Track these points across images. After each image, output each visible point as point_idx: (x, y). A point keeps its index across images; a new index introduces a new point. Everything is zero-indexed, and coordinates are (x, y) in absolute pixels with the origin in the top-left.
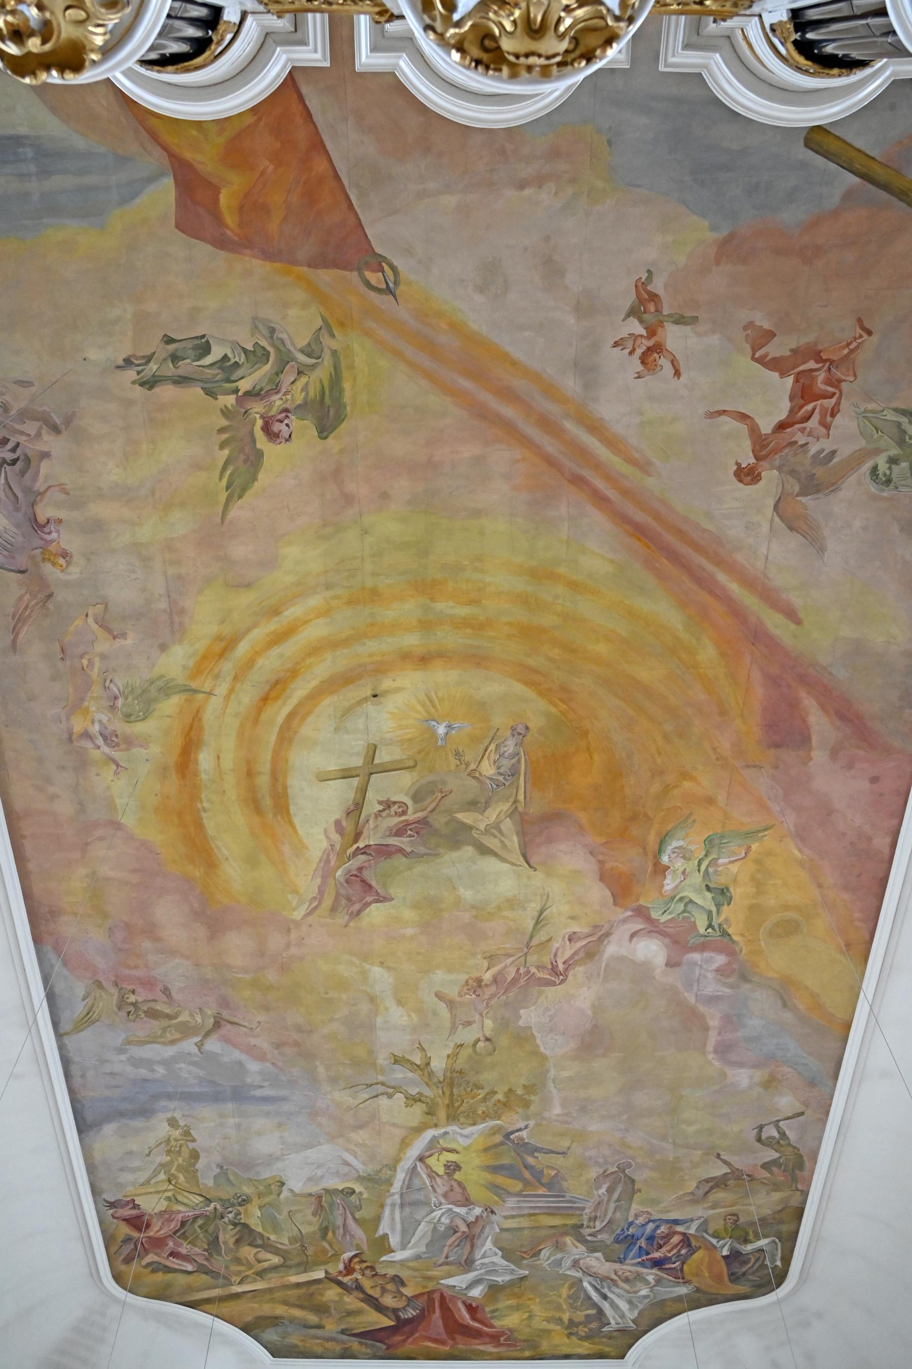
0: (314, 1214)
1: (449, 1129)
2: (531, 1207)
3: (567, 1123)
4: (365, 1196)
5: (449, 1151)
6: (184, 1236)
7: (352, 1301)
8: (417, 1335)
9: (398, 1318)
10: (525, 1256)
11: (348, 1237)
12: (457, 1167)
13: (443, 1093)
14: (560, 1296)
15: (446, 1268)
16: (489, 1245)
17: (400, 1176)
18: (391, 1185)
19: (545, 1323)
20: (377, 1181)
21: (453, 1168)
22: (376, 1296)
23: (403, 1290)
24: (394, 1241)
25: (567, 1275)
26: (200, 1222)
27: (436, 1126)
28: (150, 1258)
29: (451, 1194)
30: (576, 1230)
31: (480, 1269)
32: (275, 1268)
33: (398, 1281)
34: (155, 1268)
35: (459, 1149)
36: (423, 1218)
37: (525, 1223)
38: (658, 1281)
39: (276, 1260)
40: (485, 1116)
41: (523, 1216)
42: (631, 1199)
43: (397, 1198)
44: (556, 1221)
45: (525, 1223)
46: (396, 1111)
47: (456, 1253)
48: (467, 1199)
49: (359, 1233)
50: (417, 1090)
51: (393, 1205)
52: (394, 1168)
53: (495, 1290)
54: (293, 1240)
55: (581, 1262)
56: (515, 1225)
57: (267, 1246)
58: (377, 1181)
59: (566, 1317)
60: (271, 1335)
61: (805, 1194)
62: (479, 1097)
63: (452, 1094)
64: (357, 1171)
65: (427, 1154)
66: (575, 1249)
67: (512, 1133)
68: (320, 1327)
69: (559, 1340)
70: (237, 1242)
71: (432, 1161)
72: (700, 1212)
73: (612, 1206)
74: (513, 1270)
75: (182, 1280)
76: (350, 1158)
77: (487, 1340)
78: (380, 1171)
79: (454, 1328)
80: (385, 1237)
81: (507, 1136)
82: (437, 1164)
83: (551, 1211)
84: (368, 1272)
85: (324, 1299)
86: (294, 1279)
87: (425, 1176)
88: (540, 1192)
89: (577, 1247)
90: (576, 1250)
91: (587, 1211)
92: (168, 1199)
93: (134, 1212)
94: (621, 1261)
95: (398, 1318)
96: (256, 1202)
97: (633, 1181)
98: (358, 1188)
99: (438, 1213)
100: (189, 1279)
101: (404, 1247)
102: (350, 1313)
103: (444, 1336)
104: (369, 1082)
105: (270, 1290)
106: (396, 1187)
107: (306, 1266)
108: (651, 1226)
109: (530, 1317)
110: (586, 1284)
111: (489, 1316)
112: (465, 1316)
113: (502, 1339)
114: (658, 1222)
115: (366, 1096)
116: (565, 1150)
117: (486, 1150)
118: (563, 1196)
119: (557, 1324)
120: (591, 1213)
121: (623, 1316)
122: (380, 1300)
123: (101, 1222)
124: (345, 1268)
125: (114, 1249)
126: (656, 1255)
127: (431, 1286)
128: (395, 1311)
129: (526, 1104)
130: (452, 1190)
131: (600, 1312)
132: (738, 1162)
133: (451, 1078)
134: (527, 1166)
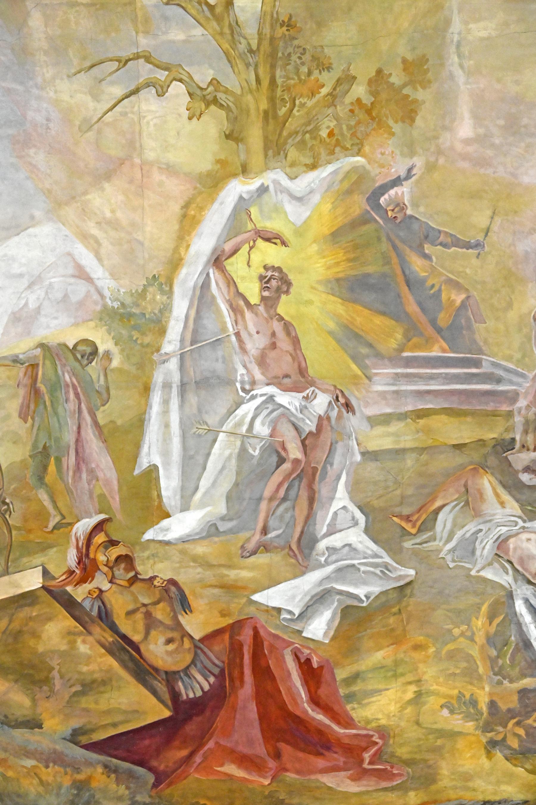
0: (24, 415)
1: (268, 178)
2: (420, 394)
3: (481, 162)
4: (115, 363)
5: (271, 238)
7: (91, 654)
8: (211, 744)
10: (408, 527)
11: (84, 476)
13: (258, 81)
14: (472, 639)
15: (262, 559)
17: (181, 306)
18: (162, 332)
19: (445, 712)
20: (136, 322)
21: (276, 283)
22: (136, 638)
23: (184, 620)
24: (169, 486)
25: (485, 580)
27: (244, 170)
29: (272, 354)
31: (327, 563)
33: (176, 596)
35: (287, 233)
36: (222, 422)
40: (336, 145)
41: (402, 417)
43: (173, 364)
46: (173, 131)
47: (282, 517)
48: (302, 371)
50: (210, 74)
51: (167, 386)
52: (165, 283)
53: (354, 620)
55: (512, 543)
56: (387, 444)
58: (136, 322)
62: (324, 91)
63: (273, 82)
64: (102, 296)
65: (228, 247)
66: (499, 510)
67: (384, 189)
68: (34, 724)
74: (386, 566)
76: (87, 259)
77: (341, 760)
78: (143, 294)
80: (153, 469)
83: (453, 403)
84: (120, 572)
85: (41, 649)
87: (224, 307)
88: (435, 352)
89: (502, 504)
91: (522, 403)
98: (104, 343)
99: (247, 409)
101: (185, 508)
102: (89, 687)
103: (260, 749)
104: (124, 54)
106: (171, 343)
109: (418, 699)
110: (520, 606)
111: (342, 691)
113: (367, 756)
115: (118, 91)
116: (480, 237)
117: (335, 236)
118: (477, 363)
119: (468, 717)
120: (528, 407)
122: (142, 648)
124: (80, 562)
127: (237, 610)
128: (170, 678)
129: (409, 112)
130: (274, 346)
133: (272, 39)
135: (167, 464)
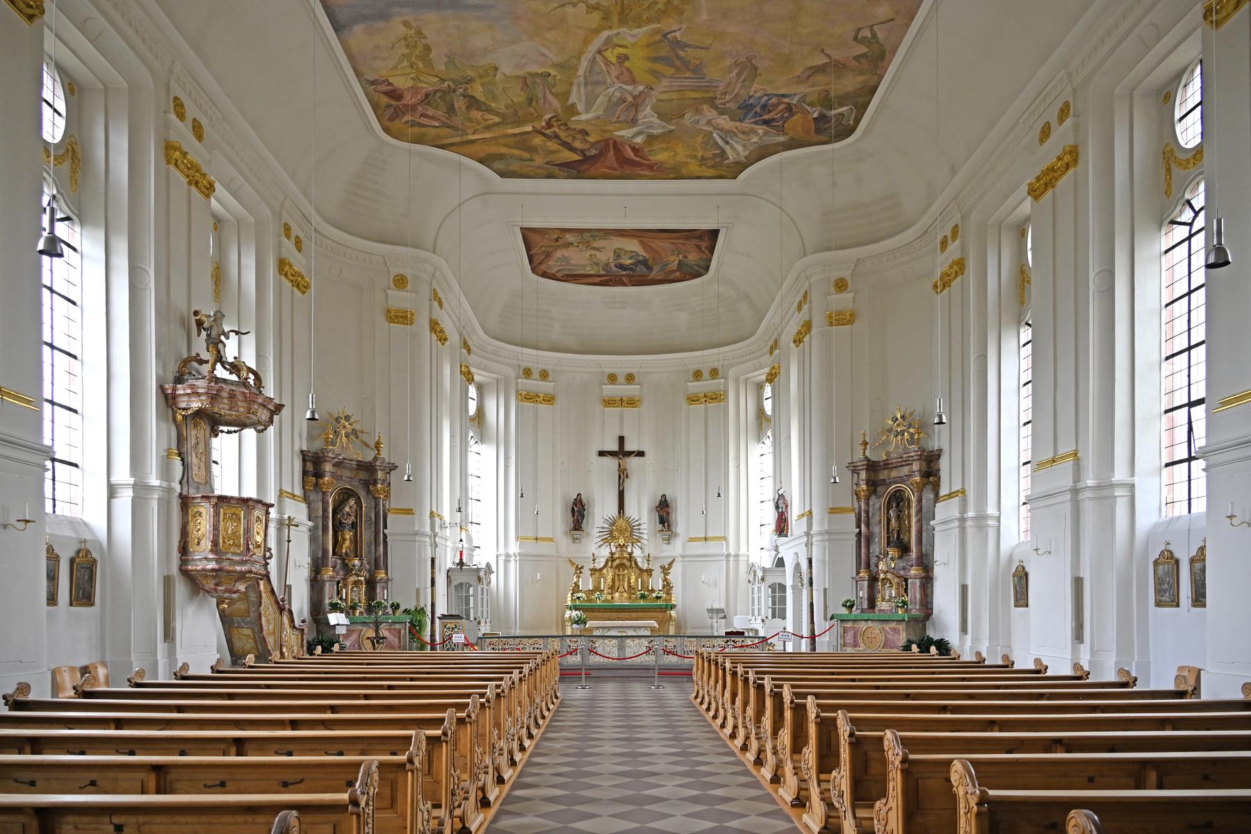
6: (428, 104)
7: (552, 145)
9: (584, 155)
12: (626, 58)
16: (648, 110)
17: (584, 65)
24: (580, 107)
26: (439, 94)
28: (408, 118)
30: (712, 102)
32: (497, 124)
33: (584, 133)
34: (414, 124)
37: (675, 96)
38: (766, 133)
39: (497, 119)
42: (753, 80)
43: (582, 79)
44: (698, 95)
45: (675, 96)
49: (556, 103)
51: (579, 84)
52: (579, 59)
53: (651, 139)
54: (507, 107)
57: (489, 110)
59: (699, 155)
60: (498, 165)
61: (881, 77)
69: (694, 168)
70: (468, 108)
71: (608, 54)
72: (802, 89)
73: (739, 85)
75: (432, 132)
79: (623, 161)
80: (574, 105)
81: (665, 36)
82: (611, 55)
86: (511, 131)
90: (709, 113)
92: (413, 79)
93: (390, 88)
94: (741, 121)
95: (584, 155)
96: (478, 81)
97: (756, 68)
100: (437, 131)
101: (587, 111)
105: (495, 138)
107: (519, 123)
108: (765, 98)
110: (715, 135)
112: (631, 154)
114: (770, 96)
121: (738, 154)
123: (367, 95)
125: (379, 112)
126: (766, 117)
127: (607, 136)
128: (582, 151)
131: (723, 151)
132: (837, 55)
134: (679, 58)
135: (580, 101)
